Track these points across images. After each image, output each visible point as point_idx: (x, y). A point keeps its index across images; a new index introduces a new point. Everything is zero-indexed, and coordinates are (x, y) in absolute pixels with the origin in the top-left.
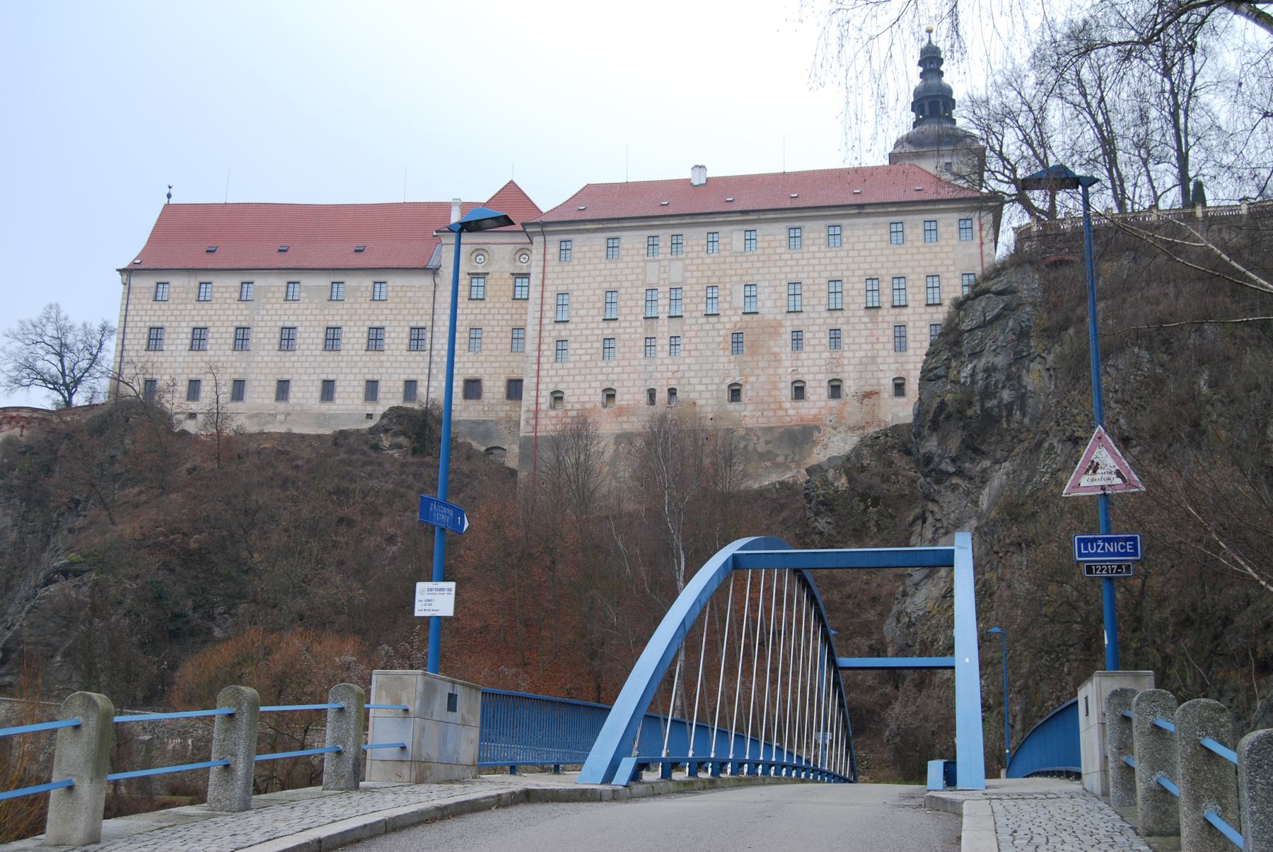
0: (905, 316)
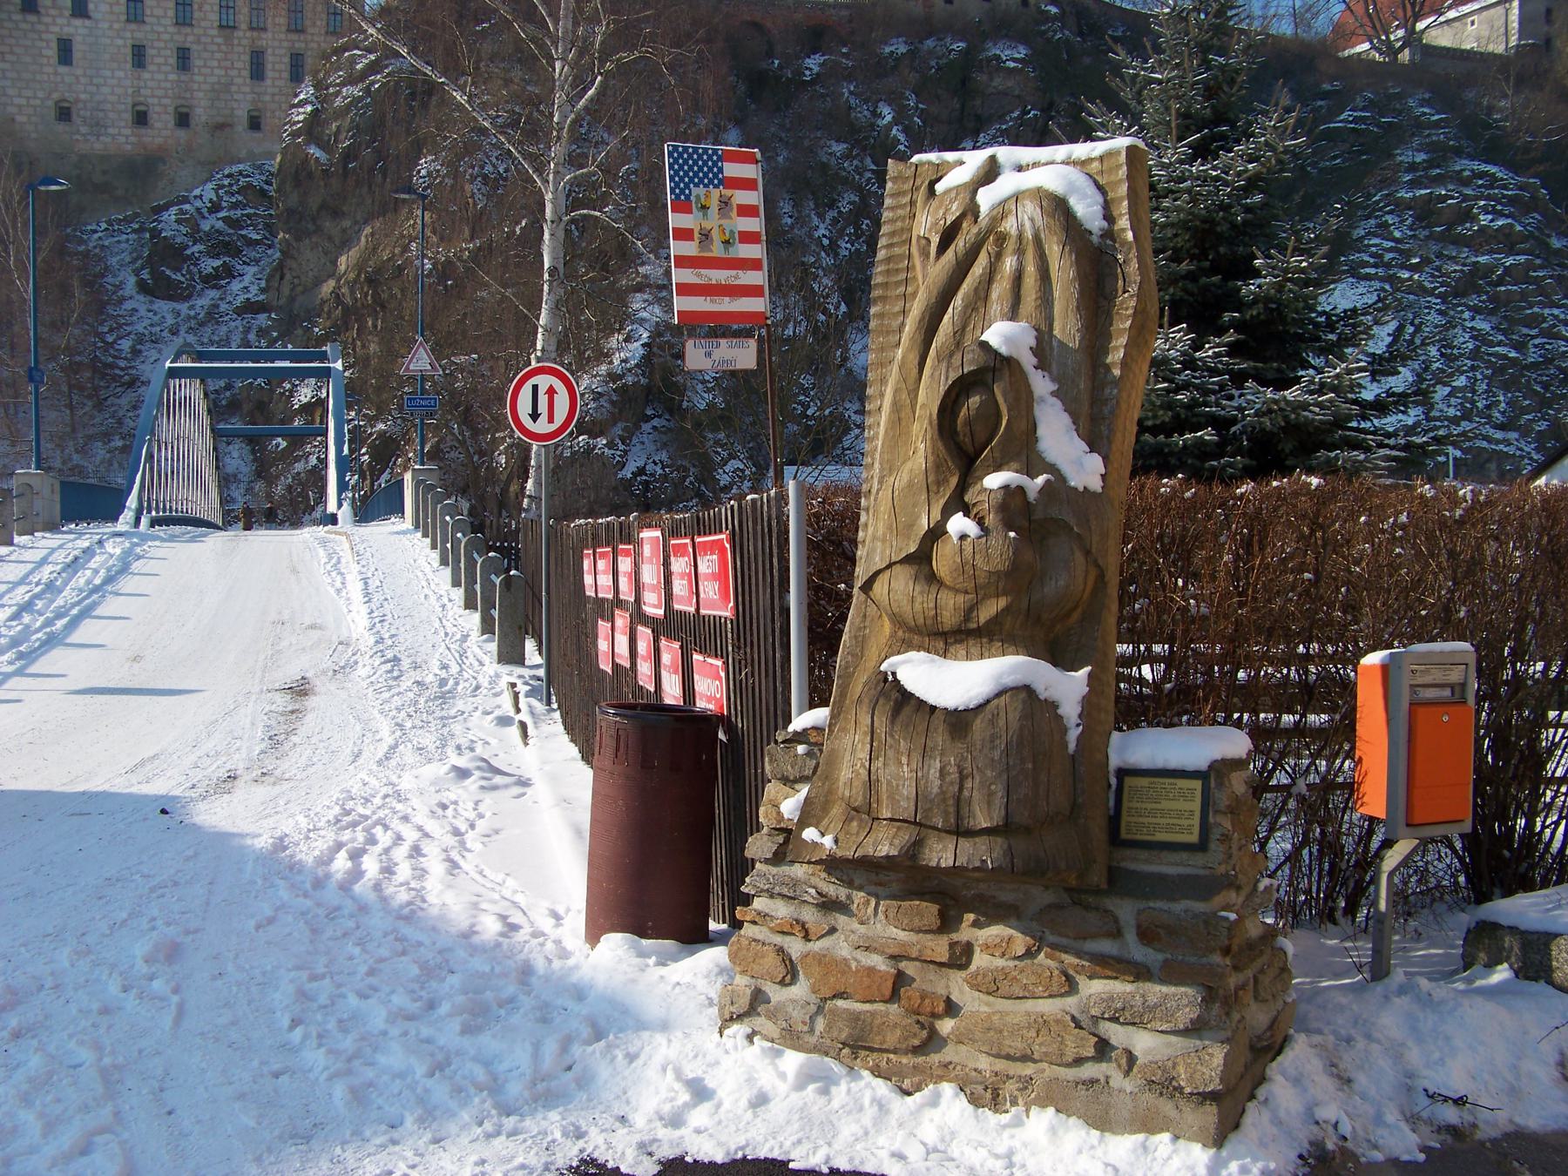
0: (266, 40)
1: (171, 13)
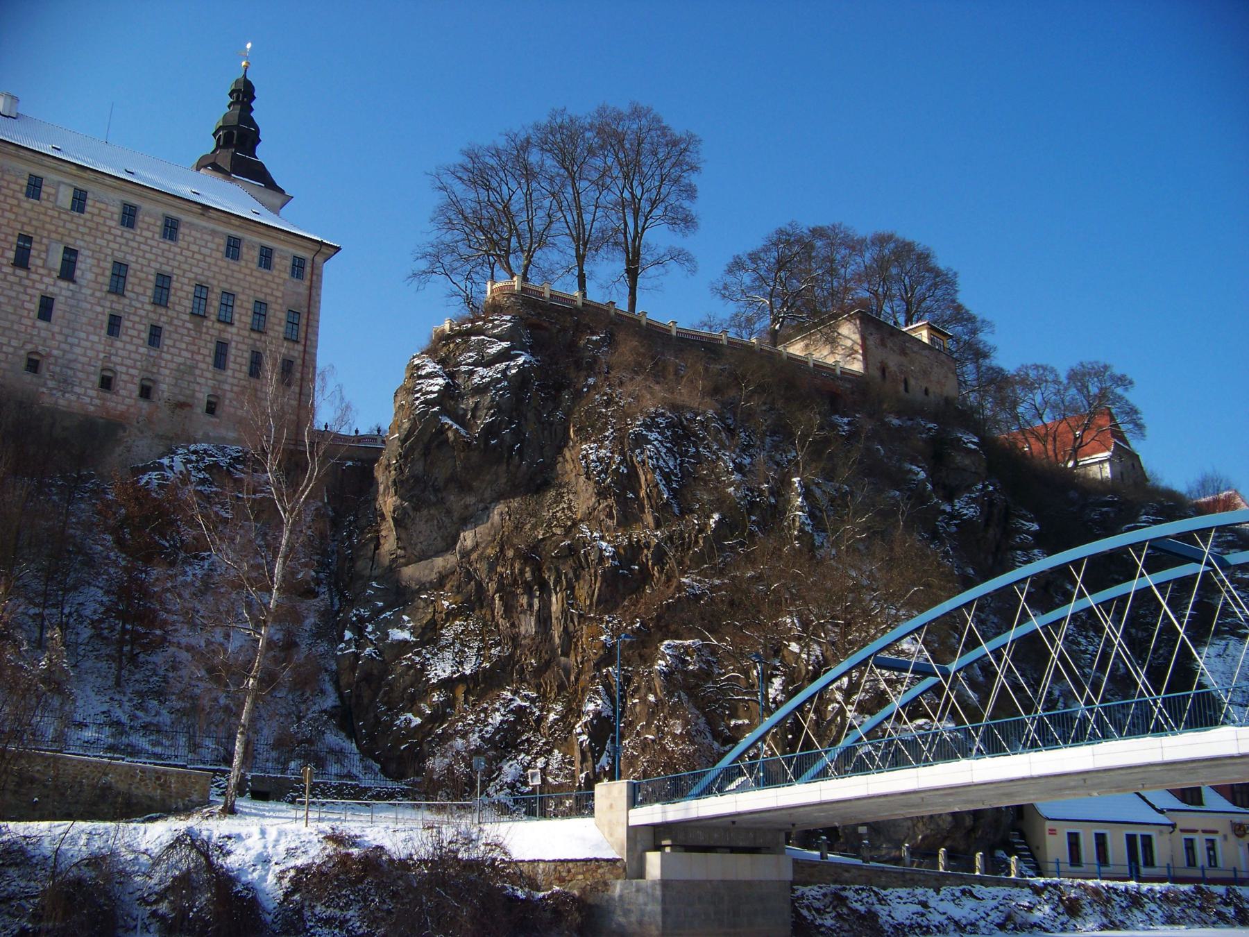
0: (231, 333)
1: (150, 293)
